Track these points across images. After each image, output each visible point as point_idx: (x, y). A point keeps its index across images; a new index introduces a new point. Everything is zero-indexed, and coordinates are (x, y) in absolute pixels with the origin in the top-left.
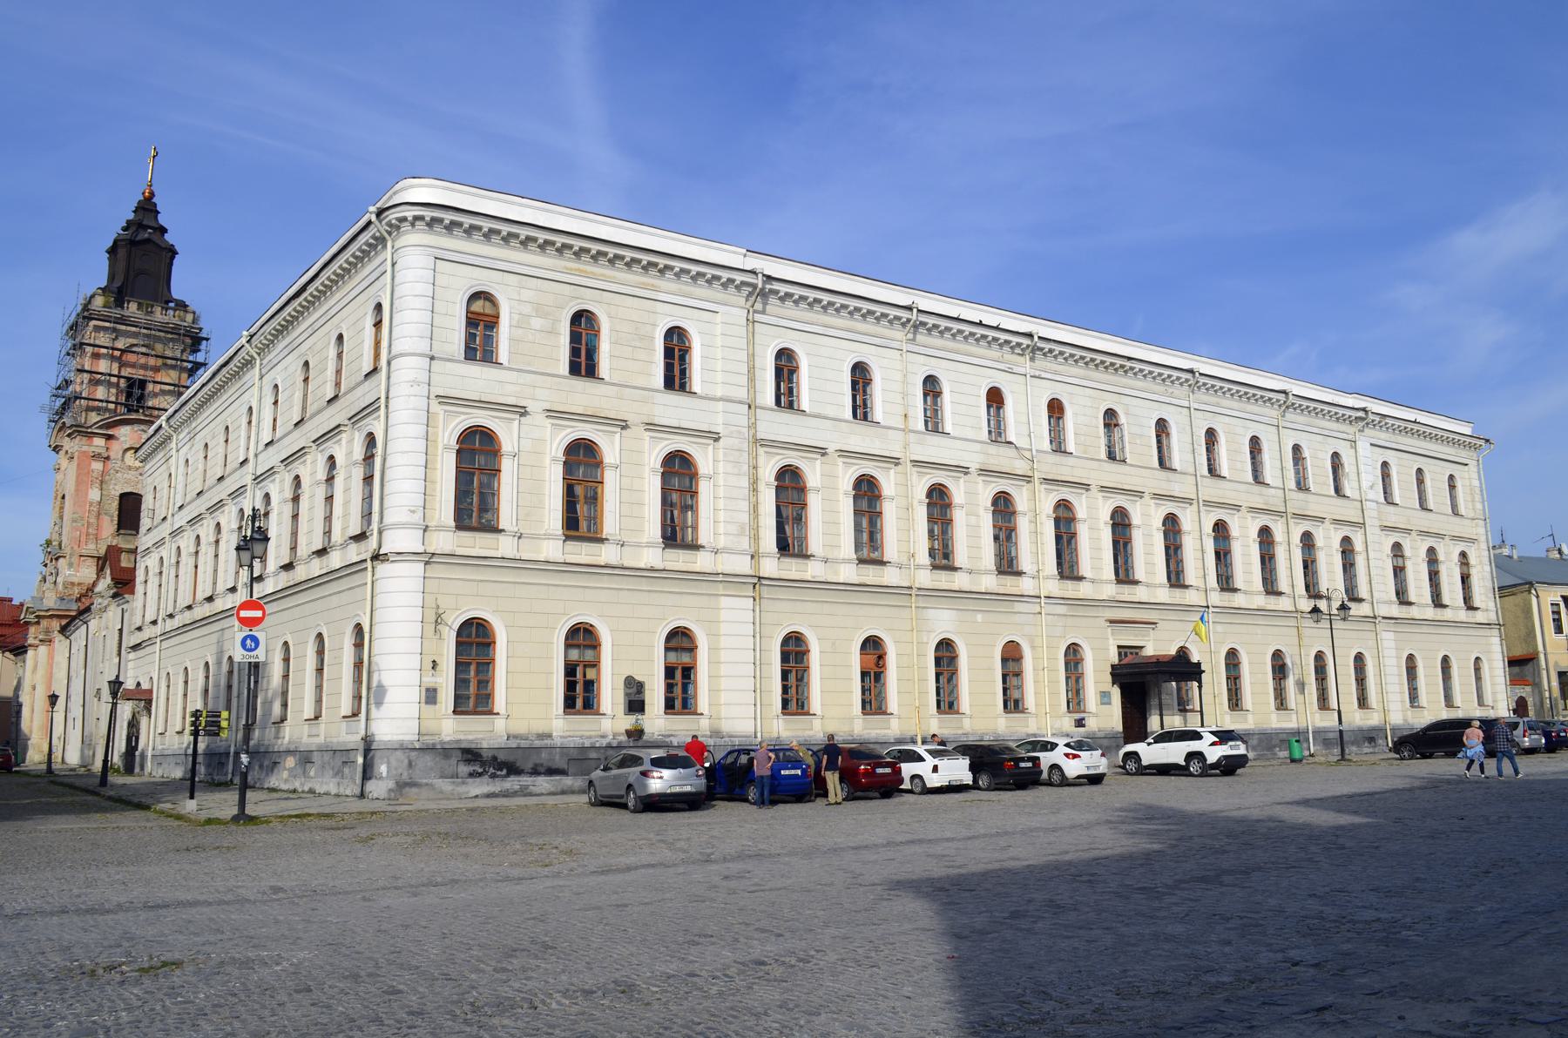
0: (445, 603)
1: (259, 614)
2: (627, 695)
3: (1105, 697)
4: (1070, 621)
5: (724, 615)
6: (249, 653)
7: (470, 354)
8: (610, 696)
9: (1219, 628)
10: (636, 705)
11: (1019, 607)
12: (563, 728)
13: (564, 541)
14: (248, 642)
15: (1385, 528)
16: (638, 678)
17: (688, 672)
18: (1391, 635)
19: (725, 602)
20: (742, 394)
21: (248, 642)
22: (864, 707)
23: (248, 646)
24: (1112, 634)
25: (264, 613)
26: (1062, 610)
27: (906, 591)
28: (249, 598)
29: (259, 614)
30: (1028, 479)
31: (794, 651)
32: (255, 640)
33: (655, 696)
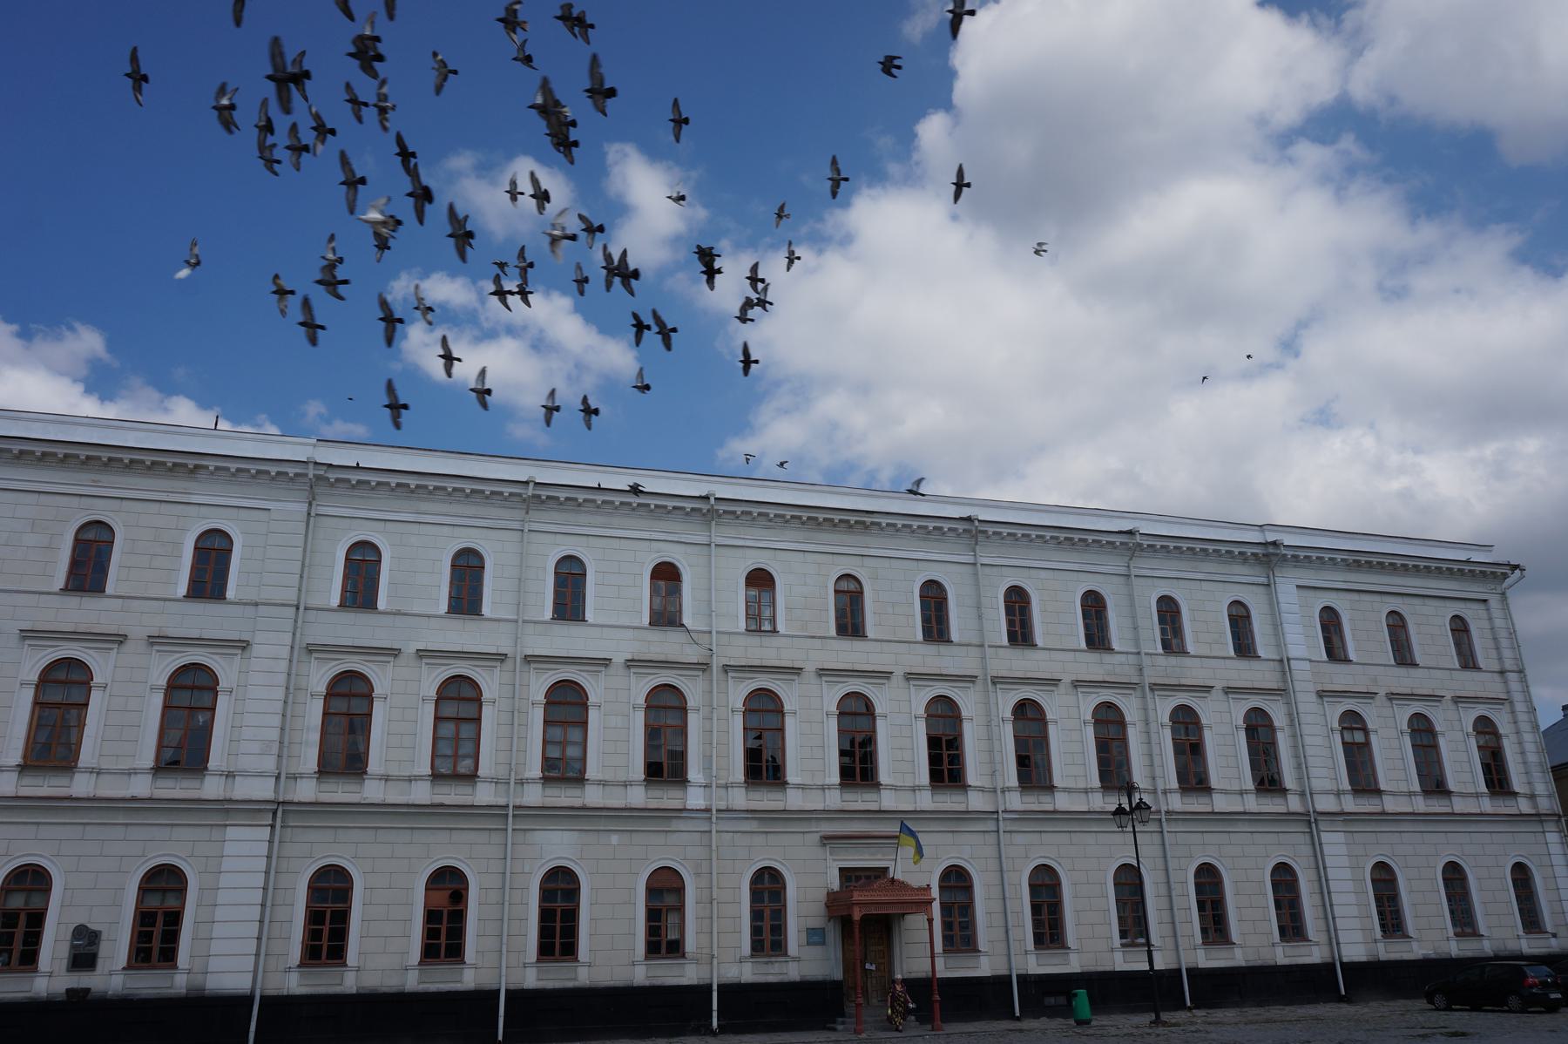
2: (73, 947)
4: (760, 839)
5: (229, 849)
9: (1018, 838)
11: (677, 825)
13: (20, 772)
15: (1321, 694)
17: (174, 918)
18: (1340, 837)
19: (231, 832)
20: (292, 598)
24: (831, 854)
26: (752, 826)
27: (497, 813)
30: (704, 667)
33: (117, 947)
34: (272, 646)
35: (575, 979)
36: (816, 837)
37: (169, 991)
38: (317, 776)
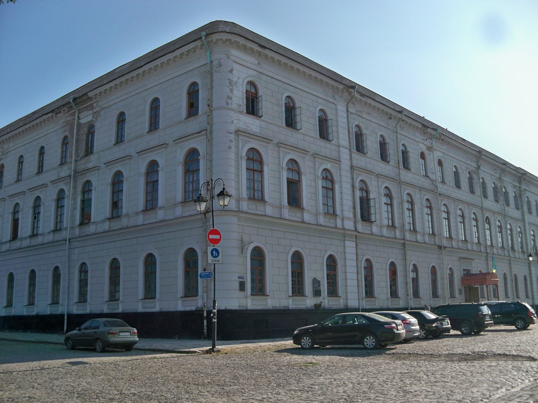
0: (246, 239)
1: (217, 237)
3: (460, 290)
6: (215, 259)
7: (248, 112)
8: (308, 288)
10: (317, 293)
12: (293, 303)
14: (214, 252)
16: (318, 279)
21: (214, 252)
22: (391, 295)
23: (214, 255)
25: (220, 237)
28: (212, 228)
29: (217, 237)
31: (369, 267)
32: (217, 251)
33: (324, 288)
34: (345, 165)
35: (421, 305)
36: (458, 258)
37: (340, 306)
38: (386, 227)
